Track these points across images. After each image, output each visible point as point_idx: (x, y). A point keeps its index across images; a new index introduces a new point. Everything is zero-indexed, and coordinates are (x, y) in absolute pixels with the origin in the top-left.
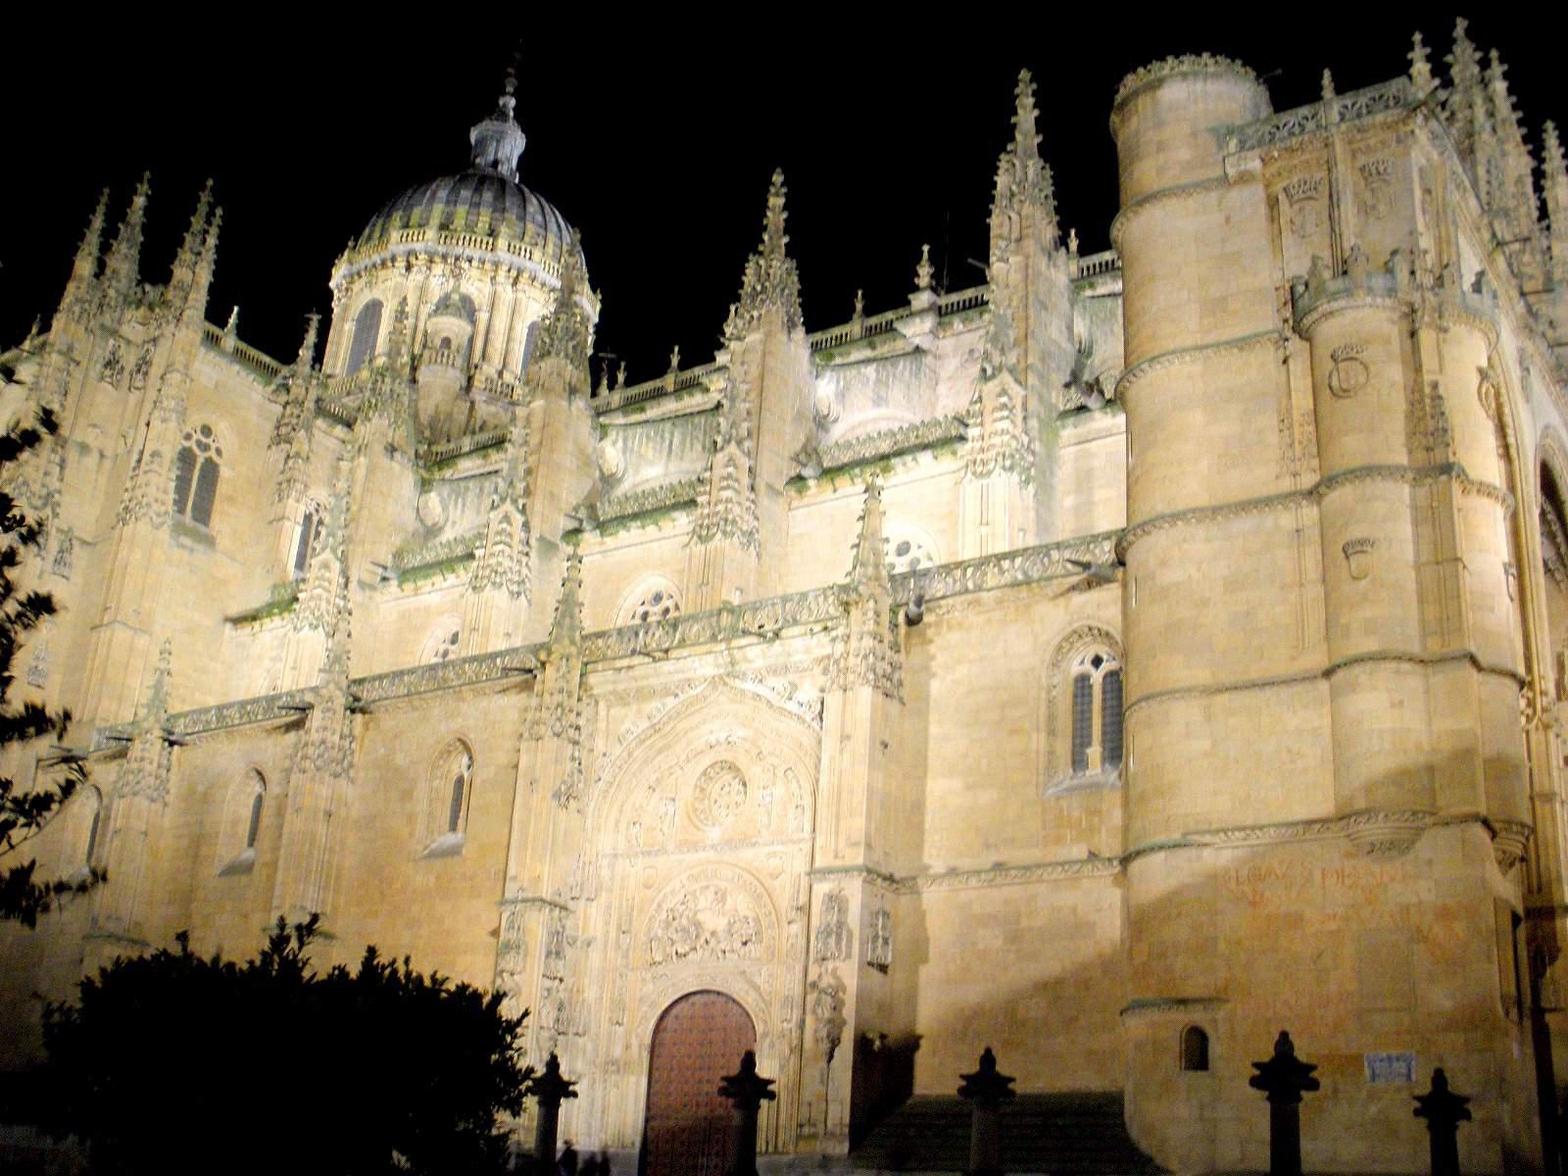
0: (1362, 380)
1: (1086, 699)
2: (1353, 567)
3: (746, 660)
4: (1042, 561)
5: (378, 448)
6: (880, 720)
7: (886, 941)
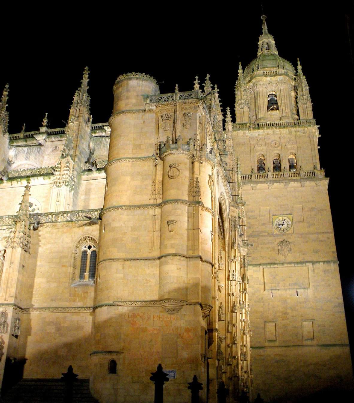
0: (178, 174)
1: (86, 258)
2: (170, 228)
4: (76, 215)
6: (23, 258)
7: (18, 328)
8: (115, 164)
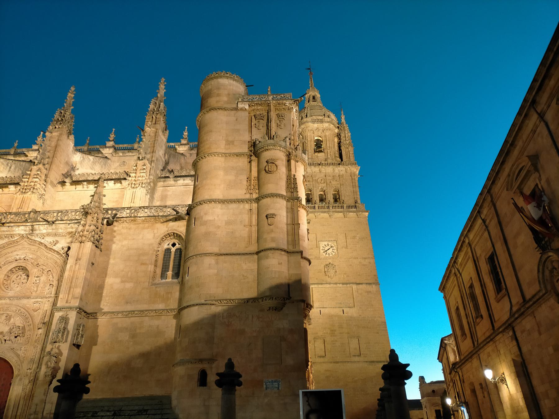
0: (275, 169)
3: (40, 230)
7: (82, 336)
8: (207, 159)
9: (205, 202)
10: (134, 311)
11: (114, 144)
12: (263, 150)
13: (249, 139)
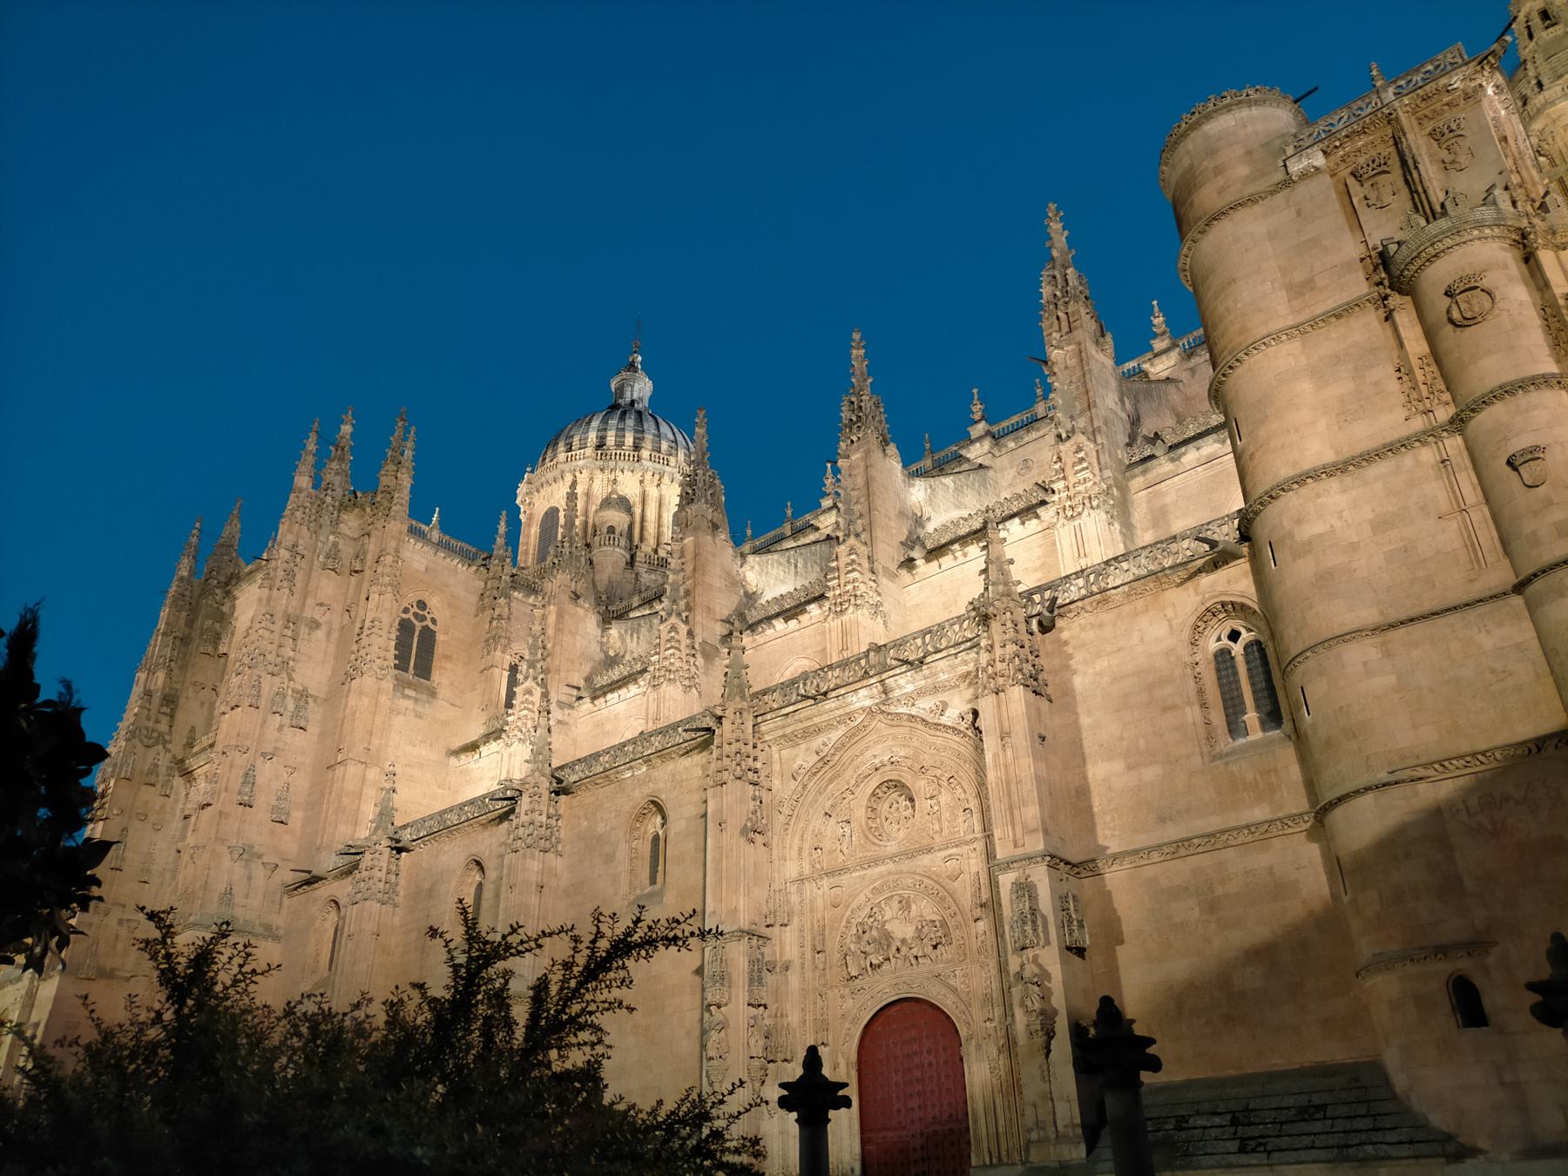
0: (1487, 304)
2: (1525, 476)
3: (900, 688)
5: (565, 597)
6: (1035, 716)
7: (1081, 925)
8: (1246, 364)
9: (1283, 487)
10: (1189, 839)
11: (987, 427)
12: (1419, 262)
13: (1360, 251)
